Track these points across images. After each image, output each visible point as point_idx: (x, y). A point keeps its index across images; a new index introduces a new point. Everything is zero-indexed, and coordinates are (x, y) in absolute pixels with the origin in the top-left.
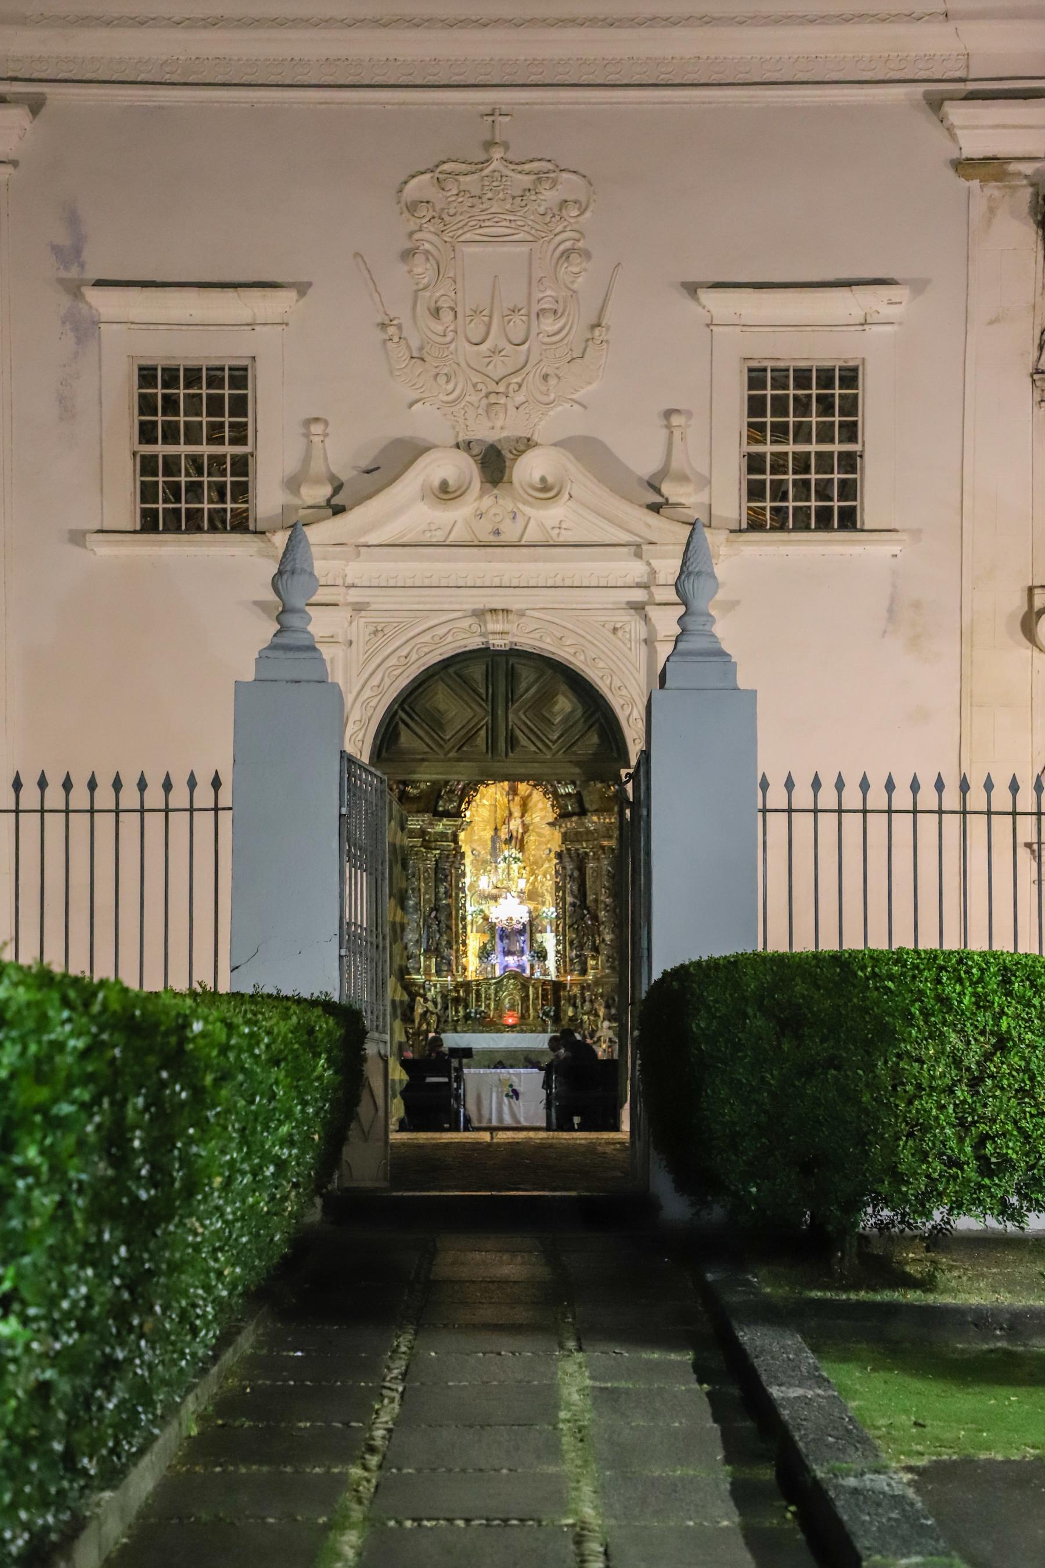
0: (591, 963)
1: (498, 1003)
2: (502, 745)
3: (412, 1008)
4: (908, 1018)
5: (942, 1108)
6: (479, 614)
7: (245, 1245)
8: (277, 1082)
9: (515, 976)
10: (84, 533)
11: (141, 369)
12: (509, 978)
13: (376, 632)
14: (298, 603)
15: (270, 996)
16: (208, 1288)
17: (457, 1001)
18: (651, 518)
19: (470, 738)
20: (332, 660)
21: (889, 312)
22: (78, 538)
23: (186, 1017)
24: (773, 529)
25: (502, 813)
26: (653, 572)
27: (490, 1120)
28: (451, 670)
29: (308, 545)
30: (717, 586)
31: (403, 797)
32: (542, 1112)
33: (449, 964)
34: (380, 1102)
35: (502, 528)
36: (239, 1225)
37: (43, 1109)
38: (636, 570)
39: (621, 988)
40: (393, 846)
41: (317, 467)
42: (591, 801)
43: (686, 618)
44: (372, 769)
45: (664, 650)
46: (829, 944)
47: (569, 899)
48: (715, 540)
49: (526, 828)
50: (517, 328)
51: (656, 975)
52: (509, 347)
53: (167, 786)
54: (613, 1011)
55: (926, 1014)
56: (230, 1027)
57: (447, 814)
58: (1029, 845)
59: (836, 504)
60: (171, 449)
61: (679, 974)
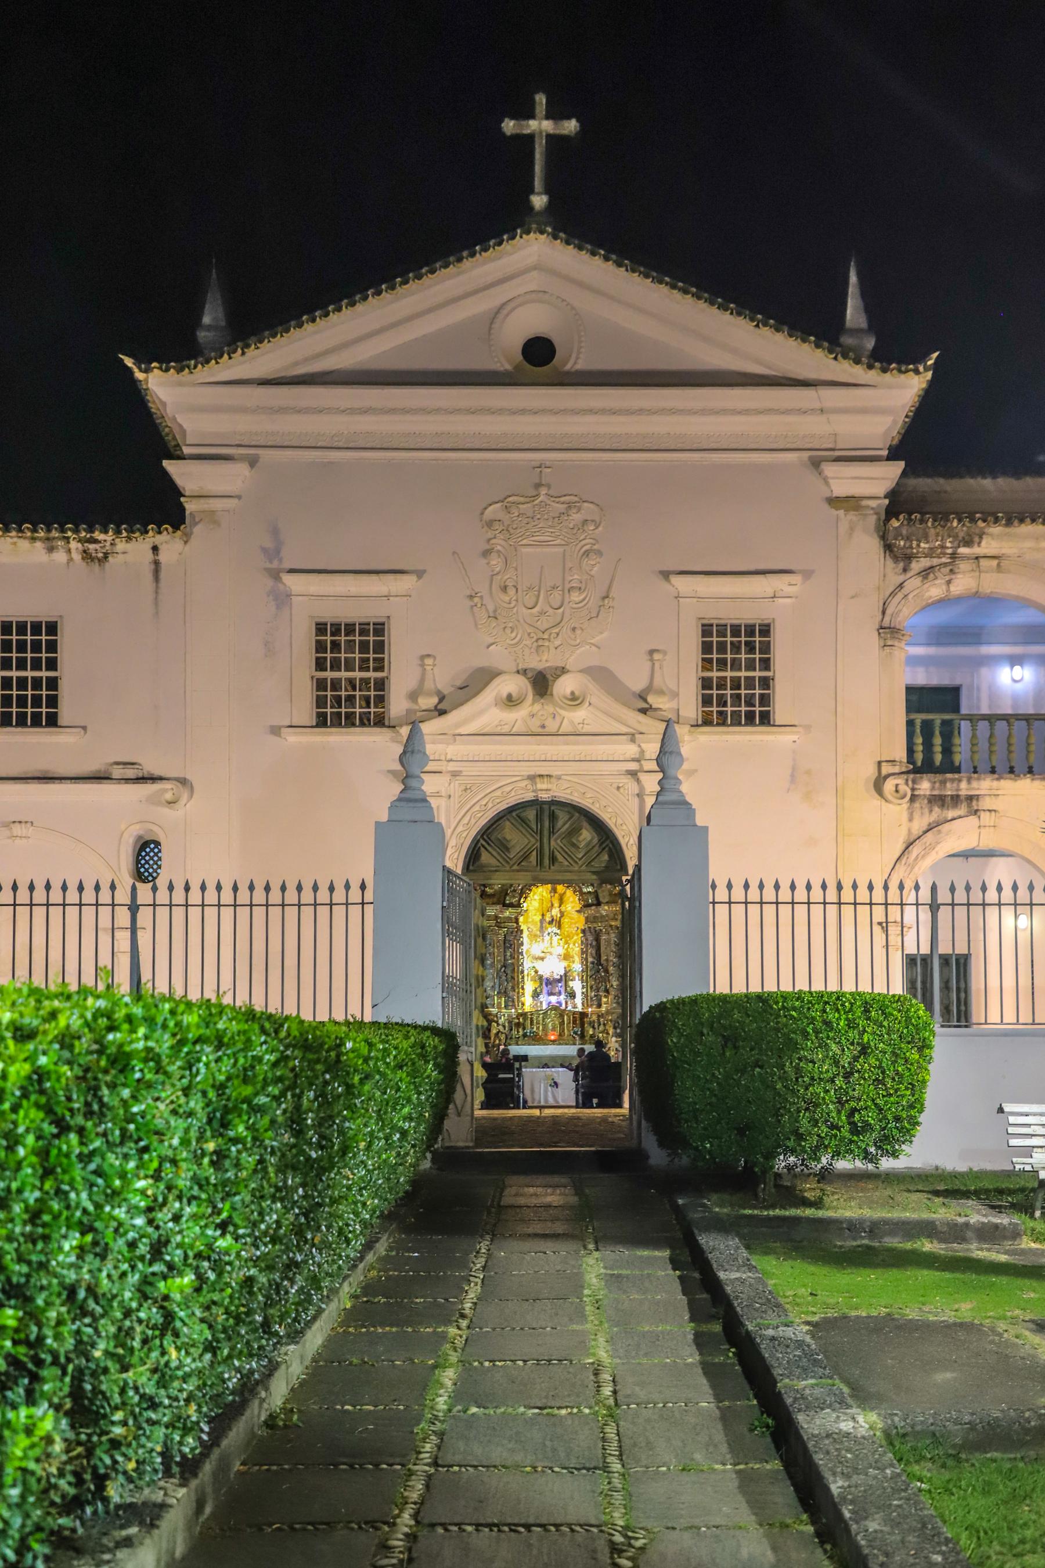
0: (604, 1000)
1: (545, 1026)
2: (546, 861)
3: (489, 1030)
4: (805, 1035)
5: (827, 1091)
6: (532, 778)
7: (380, 1185)
8: (401, 1080)
9: (555, 1008)
10: (280, 727)
11: (317, 624)
12: (551, 1010)
13: (466, 790)
14: (416, 771)
15: (397, 1024)
16: (356, 1214)
17: (518, 1025)
18: (641, 717)
19: (526, 857)
20: (438, 807)
21: (792, 590)
22: (276, 731)
23: (341, 1039)
24: (718, 724)
25: (547, 904)
26: (642, 752)
27: (540, 1102)
28: (514, 814)
29: (422, 735)
30: (682, 760)
31: (483, 895)
32: (574, 1096)
33: (513, 1001)
34: (469, 1091)
35: (546, 724)
36: (376, 1172)
37: (247, 1100)
38: (632, 750)
39: (623, 1016)
40: (477, 926)
41: (429, 685)
42: (604, 897)
43: (664, 781)
44: (464, 878)
45: (650, 801)
46: (755, 988)
47: (590, 959)
48: (682, 731)
49: (562, 914)
50: (556, 598)
51: (645, 1009)
52: (551, 611)
53: (332, 889)
54: (618, 1031)
55: (817, 1032)
56: (371, 1045)
57: (511, 905)
58: (880, 924)
59: (757, 709)
60: (336, 675)
61: (660, 1007)
